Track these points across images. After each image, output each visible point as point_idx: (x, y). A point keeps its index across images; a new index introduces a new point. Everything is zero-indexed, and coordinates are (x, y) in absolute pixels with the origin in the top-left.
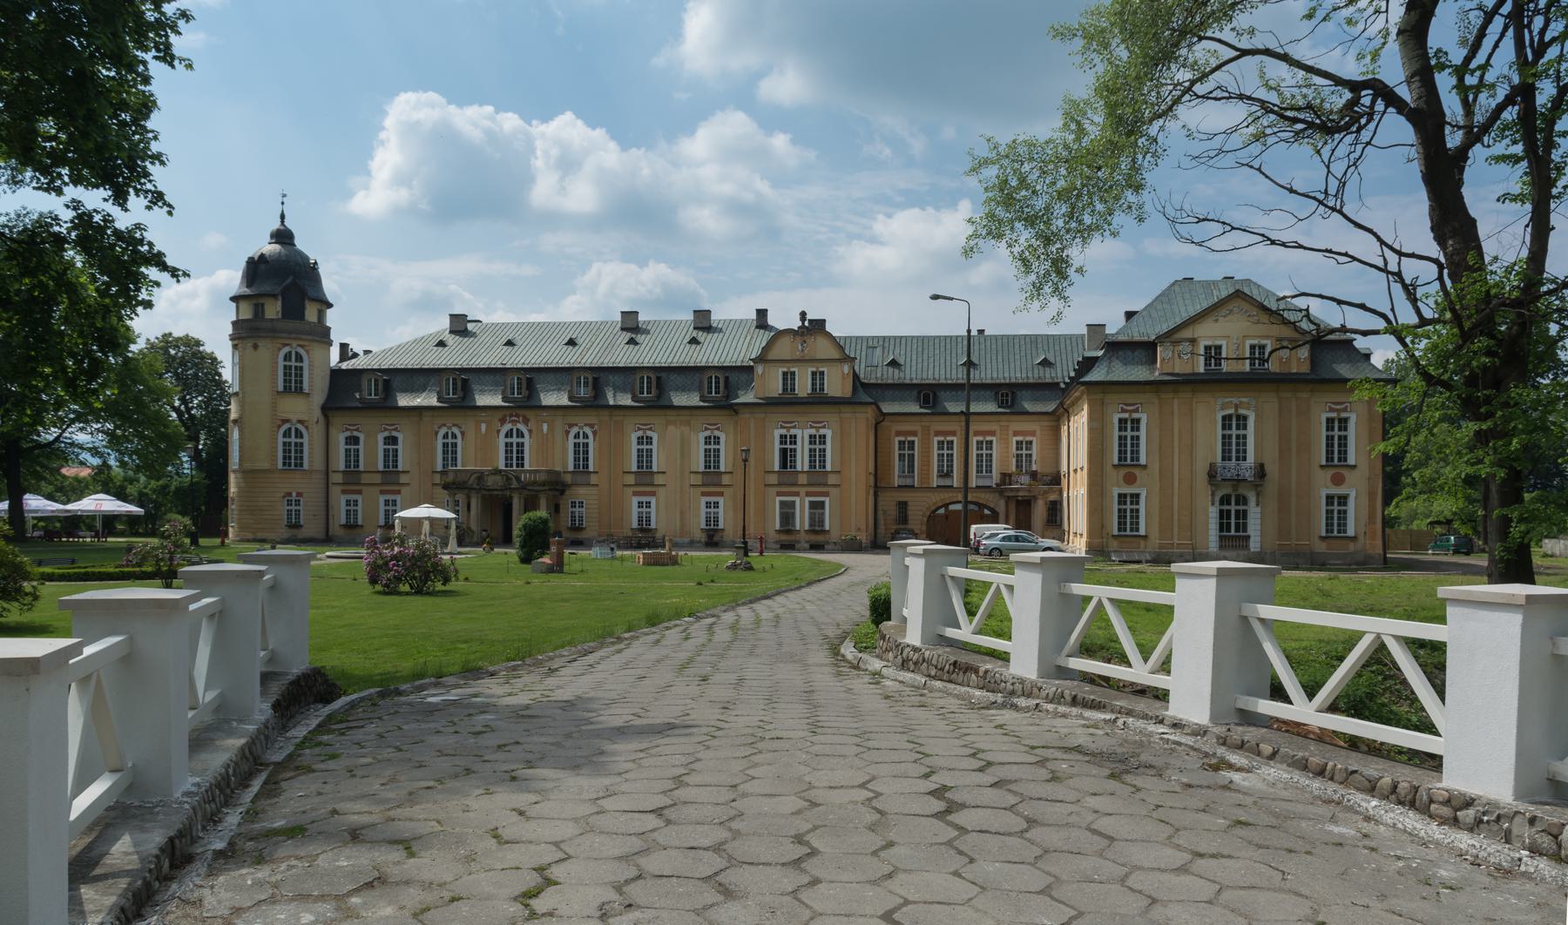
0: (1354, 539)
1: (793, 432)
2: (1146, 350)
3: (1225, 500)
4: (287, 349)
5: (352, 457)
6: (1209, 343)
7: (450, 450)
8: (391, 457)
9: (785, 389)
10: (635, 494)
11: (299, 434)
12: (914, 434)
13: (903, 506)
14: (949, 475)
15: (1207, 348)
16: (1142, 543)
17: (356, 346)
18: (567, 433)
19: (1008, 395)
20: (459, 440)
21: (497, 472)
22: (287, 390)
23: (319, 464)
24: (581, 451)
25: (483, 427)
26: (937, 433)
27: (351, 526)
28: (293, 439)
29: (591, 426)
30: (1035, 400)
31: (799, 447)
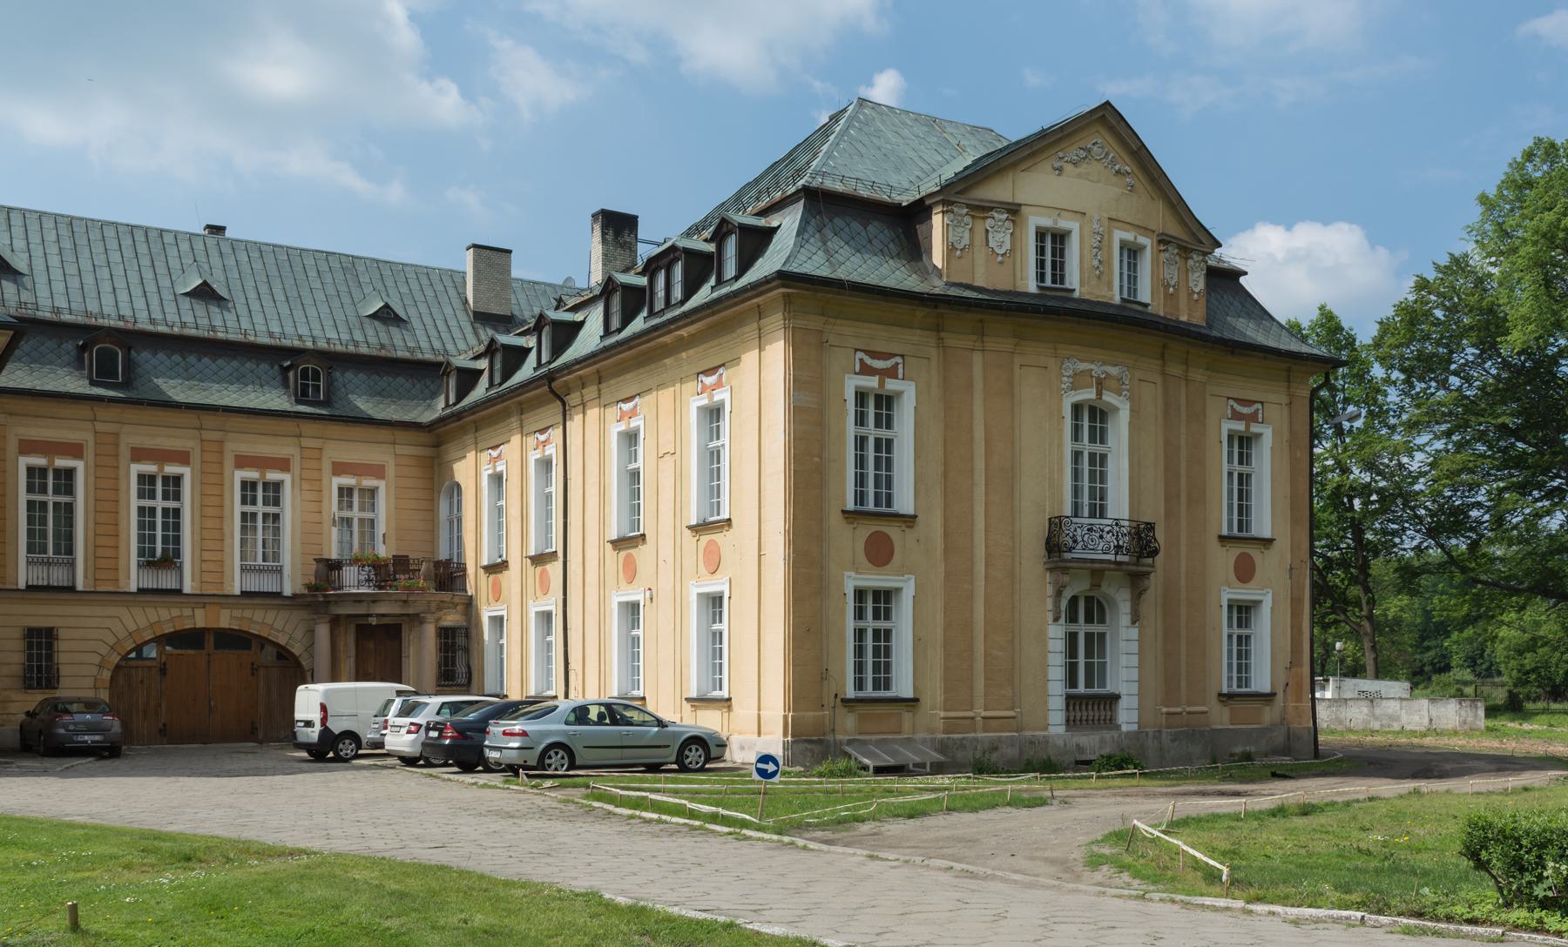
0: (1268, 697)
2: (903, 223)
6: (1046, 222)
12: (75, 451)
13: (41, 642)
14: (170, 560)
15: (1041, 235)
16: (907, 717)
19: (316, 379)
26: (139, 455)
30: (380, 394)
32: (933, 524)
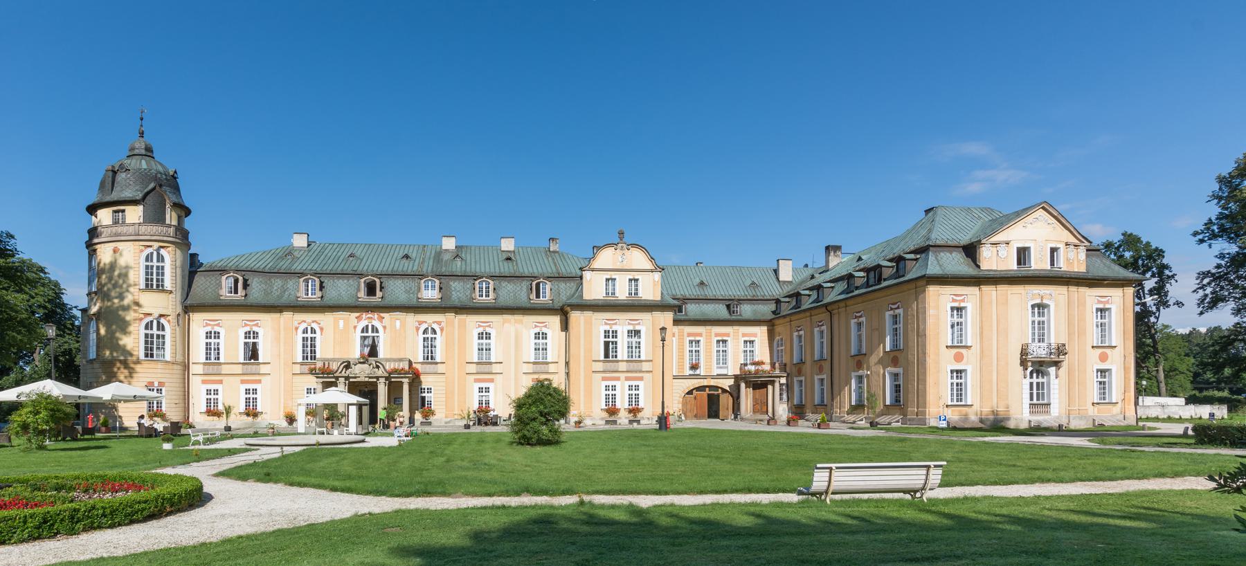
1: (614, 328)
4: (149, 250)
5: (212, 352)
9: (607, 294)
10: (477, 381)
11: (161, 327)
18: (418, 329)
20: (318, 335)
23: (179, 358)
24: (429, 345)
25: (341, 323)
28: (155, 331)
29: (439, 323)
31: (619, 340)
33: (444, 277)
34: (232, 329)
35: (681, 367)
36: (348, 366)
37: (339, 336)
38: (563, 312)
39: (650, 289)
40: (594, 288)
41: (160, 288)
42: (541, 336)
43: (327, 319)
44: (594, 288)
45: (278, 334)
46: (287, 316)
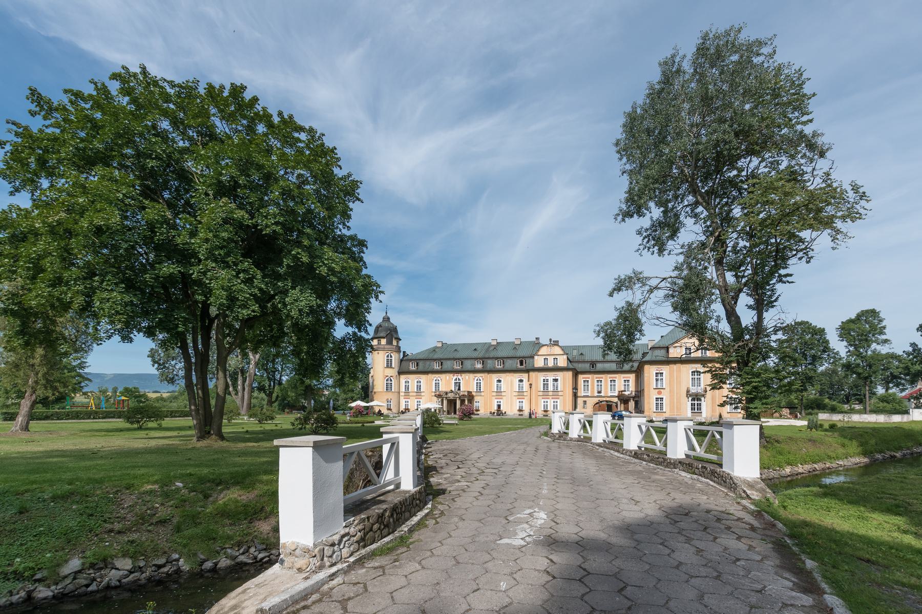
3: (693, 400)
5: (407, 388)
7: (437, 385)
8: (419, 387)
17: (408, 352)
21: (452, 391)
22: (387, 367)
27: (407, 410)
32: (668, 389)
33: (483, 360)
34: (413, 380)
35: (593, 391)
36: (446, 393)
37: (447, 383)
38: (527, 371)
39: (562, 362)
40: (539, 362)
41: (391, 367)
42: (521, 381)
43: (443, 376)
44: (539, 362)
45: (427, 382)
46: (430, 375)
